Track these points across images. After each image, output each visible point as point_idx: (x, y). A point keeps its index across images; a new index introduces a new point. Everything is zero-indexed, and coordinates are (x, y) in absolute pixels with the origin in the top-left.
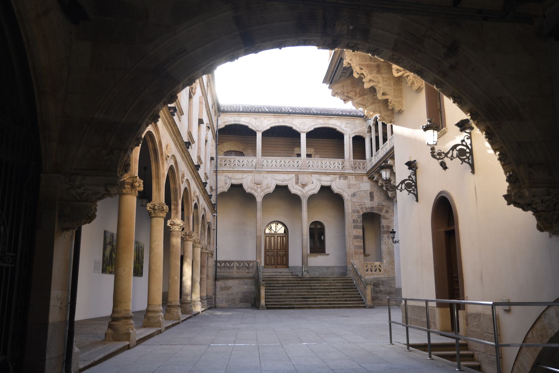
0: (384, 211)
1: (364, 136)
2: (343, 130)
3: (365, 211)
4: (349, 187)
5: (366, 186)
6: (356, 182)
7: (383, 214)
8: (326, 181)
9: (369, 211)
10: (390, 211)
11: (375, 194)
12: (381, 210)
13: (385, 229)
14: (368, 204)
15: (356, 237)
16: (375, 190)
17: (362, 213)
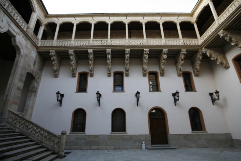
0: (37, 77)
1: (42, 24)
2: (35, 9)
3: (29, 71)
4: (26, 47)
5: (34, 54)
6: (30, 48)
7: (36, 78)
8: (14, 30)
9: (31, 72)
10: (40, 78)
11: (37, 63)
12: (36, 75)
13: (35, 89)
14: (33, 68)
15: (18, 89)
16: (38, 60)
17: (27, 71)
